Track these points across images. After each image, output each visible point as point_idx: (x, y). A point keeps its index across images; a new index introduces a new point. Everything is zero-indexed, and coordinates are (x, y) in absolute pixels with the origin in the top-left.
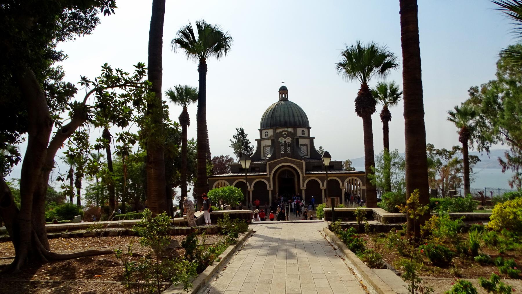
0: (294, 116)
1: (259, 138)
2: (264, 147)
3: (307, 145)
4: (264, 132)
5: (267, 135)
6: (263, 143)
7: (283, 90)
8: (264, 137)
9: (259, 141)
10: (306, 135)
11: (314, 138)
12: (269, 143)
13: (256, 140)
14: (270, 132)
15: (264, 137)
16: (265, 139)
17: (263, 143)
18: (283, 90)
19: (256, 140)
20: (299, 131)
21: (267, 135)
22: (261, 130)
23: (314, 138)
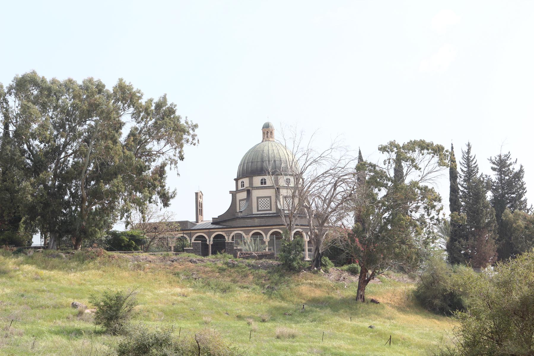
0: (275, 161)
2: (240, 201)
4: (240, 182)
5: (243, 186)
8: (240, 188)
9: (234, 194)
12: (244, 195)
13: (231, 192)
15: (240, 188)
19: (231, 192)
21: (243, 186)
22: (236, 180)
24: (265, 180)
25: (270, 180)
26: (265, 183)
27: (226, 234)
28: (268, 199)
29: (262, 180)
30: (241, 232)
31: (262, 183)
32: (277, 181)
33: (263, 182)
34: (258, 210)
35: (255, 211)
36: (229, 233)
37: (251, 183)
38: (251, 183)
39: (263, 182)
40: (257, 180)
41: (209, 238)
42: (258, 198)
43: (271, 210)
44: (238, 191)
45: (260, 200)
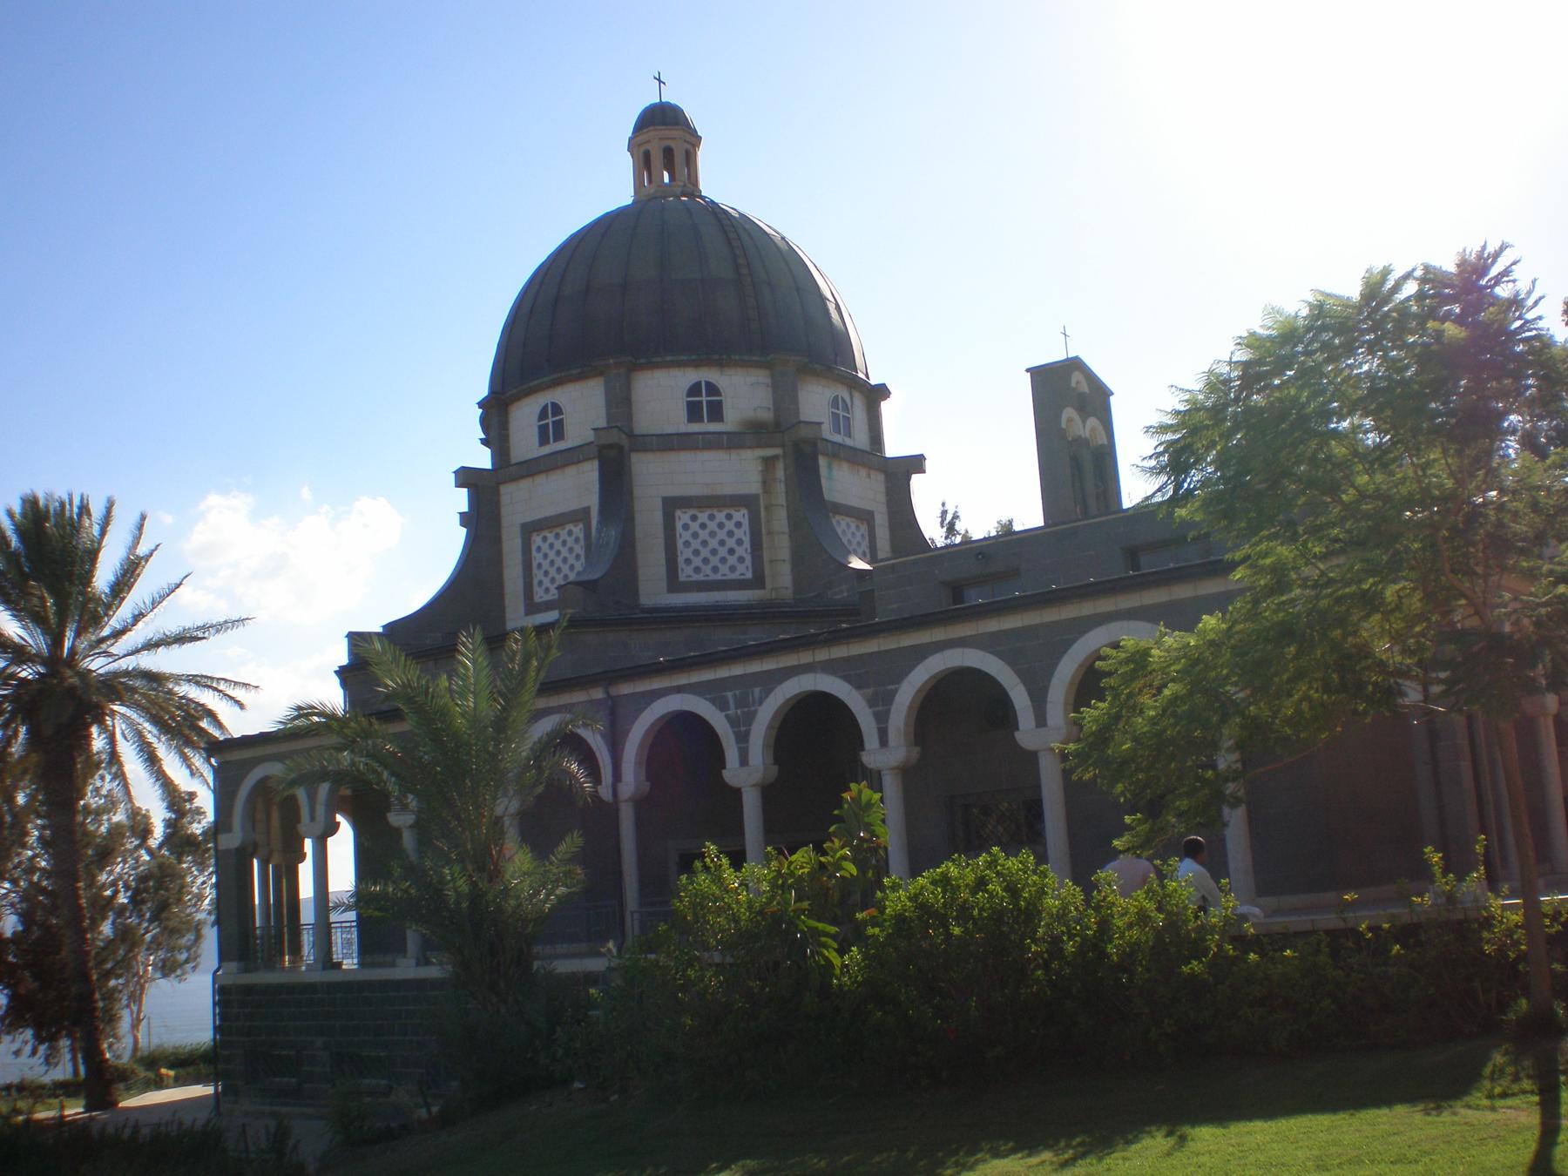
1: (482, 459)
2: (529, 529)
3: (865, 517)
5: (552, 426)
6: (523, 502)
7: (664, 137)
10: (860, 439)
11: (916, 464)
13: (466, 477)
14: (583, 406)
15: (525, 444)
16: (533, 468)
17: (523, 502)
18: (664, 137)
19: (466, 477)
20: (815, 401)
21: (552, 426)
23: (916, 464)
24: (712, 389)
25: (744, 393)
26: (716, 412)
27: (1011, 659)
28: (741, 515)
29: (694, 390)
30: (703, 707)
31: (694, 412)
32: (785, 398)
33: (703, 403)
34: (674, 585)
35: (653, 591)
36: (878, 678)
37: (620, 405)
38: (620, 405)
39: (703, 403)
40: (661, 395)
41: (1039, 699)
42: (671, 505)
43: (758, 581)
44: (507, 469)
45: (683, 517)
